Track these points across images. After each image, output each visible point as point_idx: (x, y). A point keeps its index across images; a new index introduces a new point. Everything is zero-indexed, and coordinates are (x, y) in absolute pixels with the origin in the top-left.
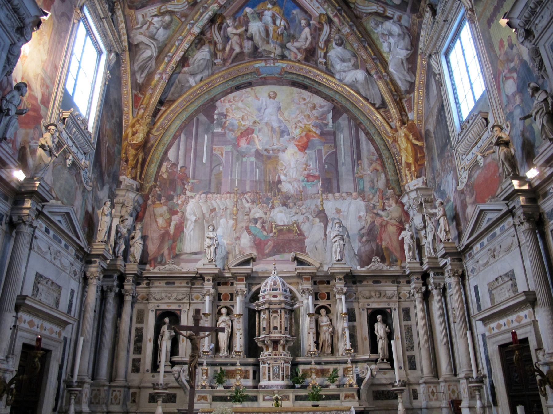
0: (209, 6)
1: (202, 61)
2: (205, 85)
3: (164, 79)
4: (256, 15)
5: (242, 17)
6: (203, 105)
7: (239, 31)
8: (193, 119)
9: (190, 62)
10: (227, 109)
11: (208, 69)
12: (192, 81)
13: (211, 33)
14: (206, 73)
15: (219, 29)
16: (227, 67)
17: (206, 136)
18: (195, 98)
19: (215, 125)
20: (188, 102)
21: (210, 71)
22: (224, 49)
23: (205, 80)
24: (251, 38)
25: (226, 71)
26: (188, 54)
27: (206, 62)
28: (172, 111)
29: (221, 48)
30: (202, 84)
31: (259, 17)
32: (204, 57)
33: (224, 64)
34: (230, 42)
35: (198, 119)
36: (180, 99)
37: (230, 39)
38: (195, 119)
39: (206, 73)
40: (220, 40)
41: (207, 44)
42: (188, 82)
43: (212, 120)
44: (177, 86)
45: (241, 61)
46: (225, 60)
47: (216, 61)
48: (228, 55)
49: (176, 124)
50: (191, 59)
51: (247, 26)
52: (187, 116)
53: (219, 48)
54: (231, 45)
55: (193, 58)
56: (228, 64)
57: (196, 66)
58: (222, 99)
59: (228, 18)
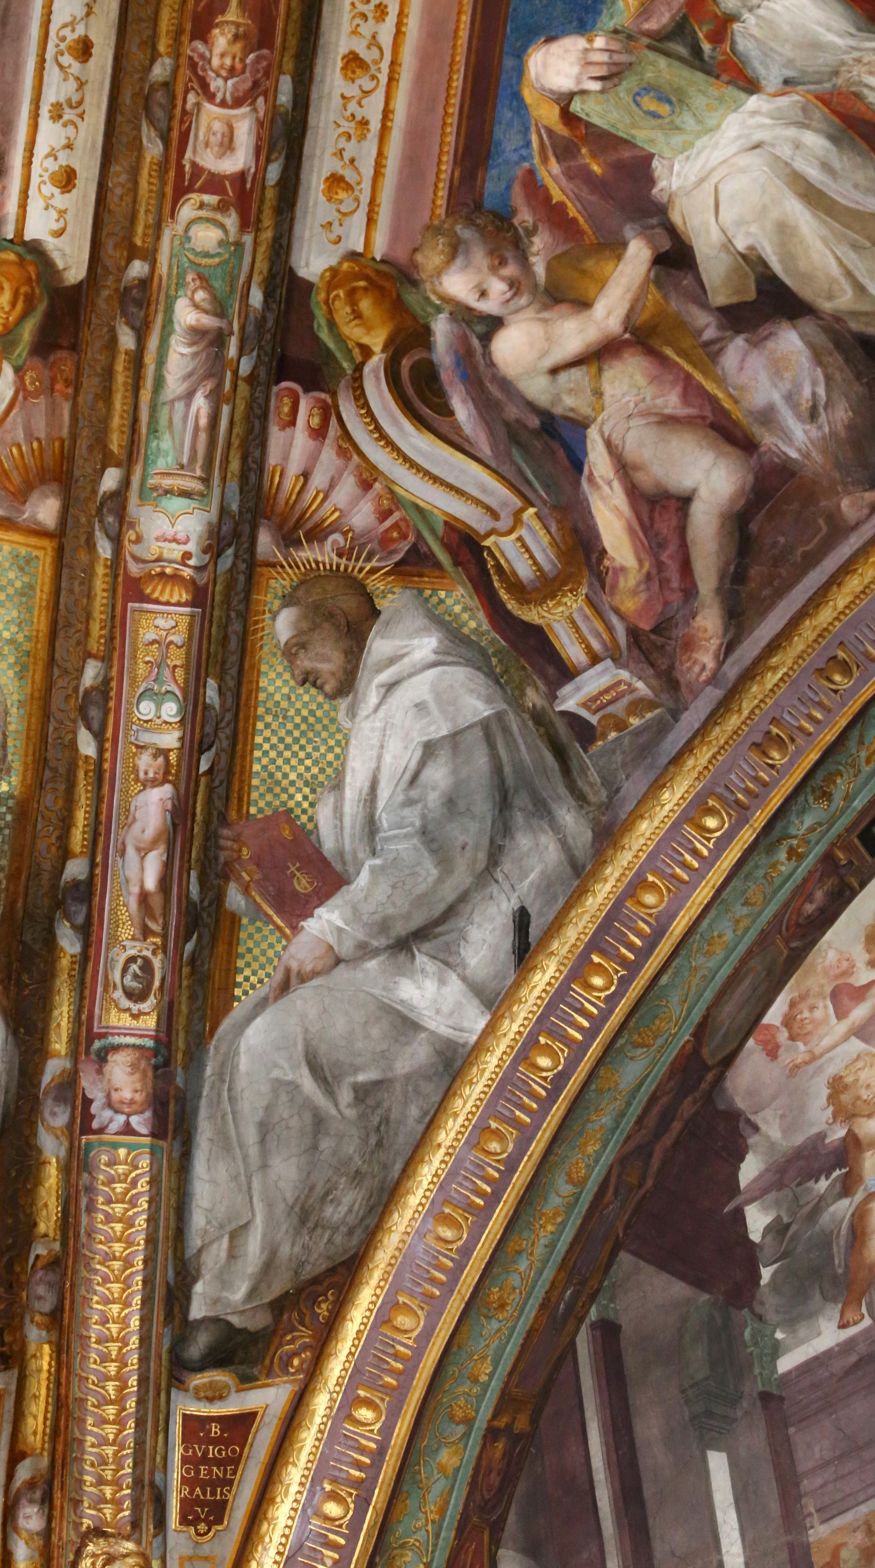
0: (150, 256)
1: (438, 775)
2: (578, 970)
3: (101, 1115)
4: (660, 69)
5: (552, 175)
6: (623, 1161)
7: (609, 312)
8: (572, 1345)
9: (328, 845)
10: (837, 1086)
11: (542, 809)
12: (434, 997)
13: (369, 477)
14: (537, 855)
15: (421, 395)
16: (713, 694)
17: (718, 1464)
18: (537, 1147)
19: (769, 1303)
20: (483, 1215)
21: (569, 817)
22: (581, 549)
23: (555, 927)
24: (769, 301)
25: (719, 734)
26: (273, 784)
27: (481, 761)
28: (357, 1375)
29: (546, 556)
30: (545, 976)
31: (696, 59)
32: (444, 730)
33: (669, 681)
34: (598, 460)
35: (608, 1332)
36: (402, 1223)
37: (581, 425)
38: (584, 1345)
39: (537, 855)
40: (498, 493)
41: (393, 600)
42: (405, 1024)
43: (720, 1262)
44: (319, 1123)
45: (812, 560)
46: (652, 646)
47: (571, 700)
48: (655, 577)
49: (438, 1487)
50: (324, 815)
51: (654, 214)
52: (512, 1349)
53: (524, 570)
54: (624, 468)
55: (337, 785)
56: (707, 659)
57: (402, 846)
58: (774, 1015)
59: (430, 259)
